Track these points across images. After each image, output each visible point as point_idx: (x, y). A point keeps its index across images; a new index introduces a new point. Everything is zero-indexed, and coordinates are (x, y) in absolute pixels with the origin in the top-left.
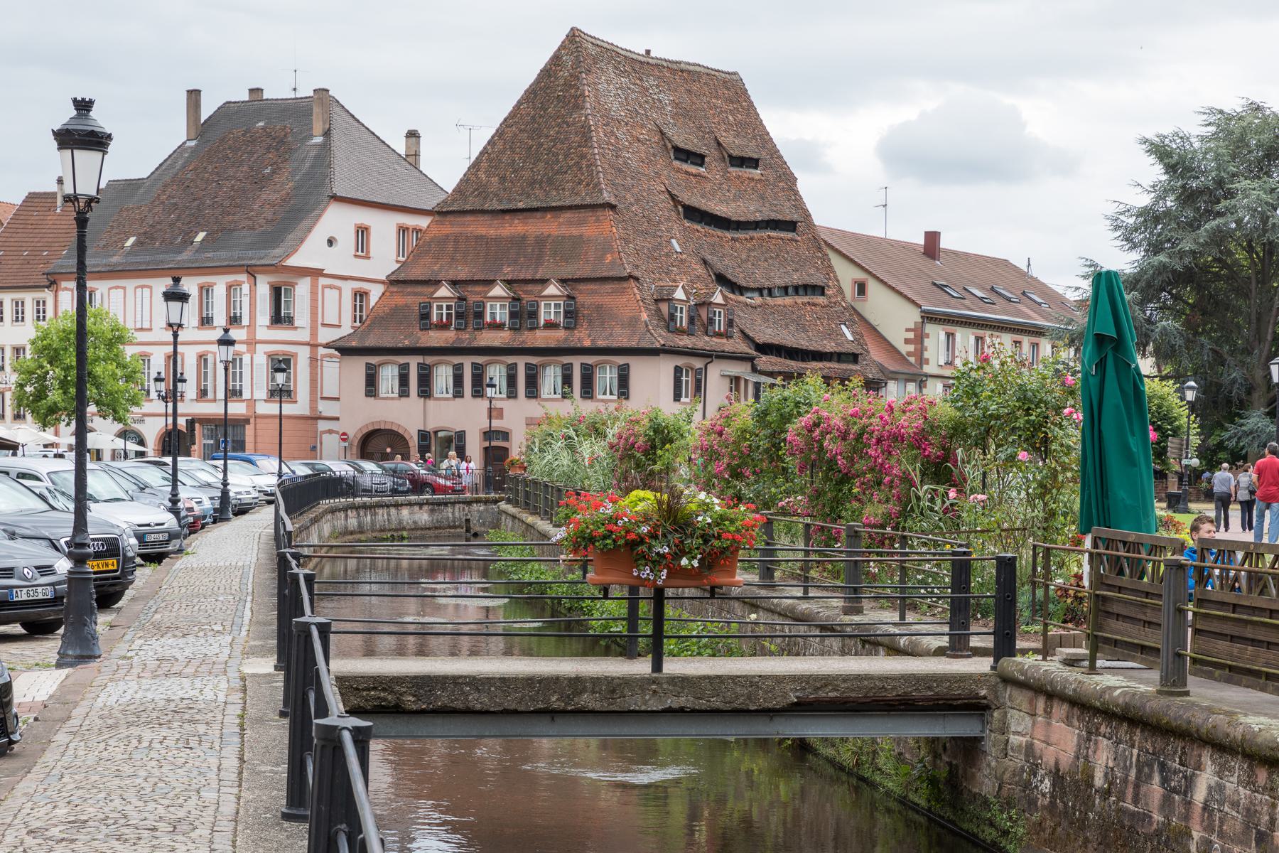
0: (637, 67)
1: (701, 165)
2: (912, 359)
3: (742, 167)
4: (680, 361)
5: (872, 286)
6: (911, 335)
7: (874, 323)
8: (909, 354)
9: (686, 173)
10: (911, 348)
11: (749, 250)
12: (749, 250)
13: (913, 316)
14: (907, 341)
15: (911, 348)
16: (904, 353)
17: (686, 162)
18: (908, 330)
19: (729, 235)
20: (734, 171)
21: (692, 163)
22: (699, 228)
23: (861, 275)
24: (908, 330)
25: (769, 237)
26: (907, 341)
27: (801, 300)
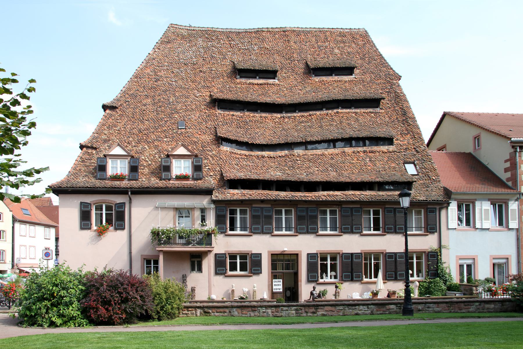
0: (234, 36)
1: (274, 79)
2: (510, 184)
3: (331, 75)
4: (89, 199)
5: (485, 138)
6: (508, 165)
7: (485, 163)
8: (508, 179)
9: (250, 84)
10: (509, 175)
11: (302, 122)
12: (302, 122)
13: (506, 150)
14: (506, 170)
15: (509, 175)
16: (505, 180)
17: (255, 78)
18: (506, 161)
19: (279, 115)
20: (317, 79)
21: (260, 78)
22: (238, 113)
23: (475, 132)
24: (506, 161)
25: (337, 112)
26: (506, 170)
27: (349, 150)
